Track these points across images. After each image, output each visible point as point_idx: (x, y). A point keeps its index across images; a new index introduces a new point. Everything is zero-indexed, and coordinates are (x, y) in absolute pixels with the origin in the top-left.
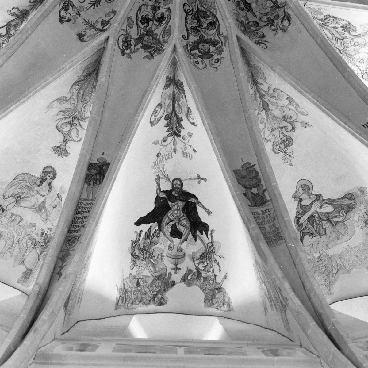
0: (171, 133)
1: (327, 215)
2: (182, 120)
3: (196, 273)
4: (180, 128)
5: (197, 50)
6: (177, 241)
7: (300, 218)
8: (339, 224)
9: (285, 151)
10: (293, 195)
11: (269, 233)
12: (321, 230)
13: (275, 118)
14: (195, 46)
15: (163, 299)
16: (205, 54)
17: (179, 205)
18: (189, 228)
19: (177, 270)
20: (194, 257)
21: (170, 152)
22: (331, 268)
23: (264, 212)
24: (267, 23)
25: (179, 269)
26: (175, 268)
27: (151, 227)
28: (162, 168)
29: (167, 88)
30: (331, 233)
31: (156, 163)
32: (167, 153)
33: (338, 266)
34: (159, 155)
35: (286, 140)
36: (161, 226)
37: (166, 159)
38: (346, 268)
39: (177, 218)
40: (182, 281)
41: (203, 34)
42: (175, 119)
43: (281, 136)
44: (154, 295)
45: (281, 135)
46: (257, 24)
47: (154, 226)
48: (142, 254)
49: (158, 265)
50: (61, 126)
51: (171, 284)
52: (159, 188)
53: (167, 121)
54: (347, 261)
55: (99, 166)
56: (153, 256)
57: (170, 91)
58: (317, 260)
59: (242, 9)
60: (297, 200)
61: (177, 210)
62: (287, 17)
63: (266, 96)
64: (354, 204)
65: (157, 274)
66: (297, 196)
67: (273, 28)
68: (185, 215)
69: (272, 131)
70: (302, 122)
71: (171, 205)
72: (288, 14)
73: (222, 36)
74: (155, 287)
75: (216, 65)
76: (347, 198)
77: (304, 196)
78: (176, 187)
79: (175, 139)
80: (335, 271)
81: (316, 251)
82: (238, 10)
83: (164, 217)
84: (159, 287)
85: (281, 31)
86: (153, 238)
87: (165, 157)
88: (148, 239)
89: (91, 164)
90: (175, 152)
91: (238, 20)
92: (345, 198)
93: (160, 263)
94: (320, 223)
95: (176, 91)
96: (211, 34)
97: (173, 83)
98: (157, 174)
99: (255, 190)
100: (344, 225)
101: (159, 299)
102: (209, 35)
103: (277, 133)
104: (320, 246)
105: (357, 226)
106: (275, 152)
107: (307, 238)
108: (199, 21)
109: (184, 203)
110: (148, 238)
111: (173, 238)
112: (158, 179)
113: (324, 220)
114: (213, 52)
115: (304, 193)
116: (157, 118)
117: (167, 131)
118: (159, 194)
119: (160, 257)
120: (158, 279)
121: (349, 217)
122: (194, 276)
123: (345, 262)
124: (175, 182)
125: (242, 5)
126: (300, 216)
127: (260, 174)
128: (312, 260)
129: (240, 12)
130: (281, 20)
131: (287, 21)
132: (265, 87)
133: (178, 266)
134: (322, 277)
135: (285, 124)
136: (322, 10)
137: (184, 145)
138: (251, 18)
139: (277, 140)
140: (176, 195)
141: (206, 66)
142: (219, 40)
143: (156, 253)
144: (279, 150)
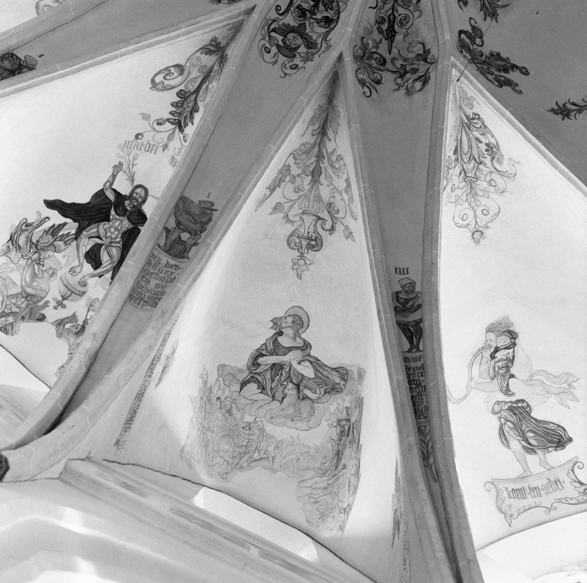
0: (175, 120)
1: (301, 378)
2: (197, 111)
3: (80, 327)
4: (188, 121)
5: (282, 38)
6: (88, 268)
7: (263, 355)
8: (307, 402)
9: (303, 252)
10: (275, 319)
11: (148, 290)
12: (280, 393)
13: (319, 198)
14: (283, 30)
15: (12, 328)
16: (287, 49)
17: (124, 223)
18: (114, 262)
19: (60, 305)
20: (93, 306)
21: (157, 144)
22: (254, 449)
23: (169, 265)
24: (397, 70)
25: (64, 307)
26: (59, 301)
27: (65, 224)
28: (133, 157)
29: (206, 54)
30: (289, 405)
31: (129, 143)
32: (152, 143)
33: (265, 454)
34: (140, 137)
35: (313, 238)
36: (81, 234)
37: (147, 149)
38: (273, 464)
39: (109, 240)
40: (55, 324)
41: (307, 25)
42: (191, 104)
43: (312, 229)
44: (5, 312)
45: (312, 227)
46: (383, 62)
47: (72, 226)
48: (29, 248)
49: (40, 280)
50: (43, 7)
51: (39, 317)
52: (111, 182)
53: (179, 99)
54: (283, 456)
55: (20, 65)
56: (42, 263)
57: (208, 60)
58: (244, 425)
59: (380, 31)
60: (276, 329)
61: (116, 229)
62: (425, 79)
63: (326, 161)
64: (342, 388)
65: (30, 291)
66: (279, 324)
67: (399, 81)
68: (121, 243)
69: (303, 213)
70: (347, 228)
71: (113, 216)
72: (429, 76)
73: (326, 43)
74: (14, 304)
75: (289, 71)
76: (338, 373)
77: (289, 332)
78: (135, 198)
79: (174, 132)
80: (256, 456)
81: (253, 413)
82: (375, 28)
83: (92, 226)
84: (20, 308)
85: (405, 91)
86: (59, 240)
87: (146, 146)
88: (51, 237)
89: (13, 54)
90: (164, 150)
91: (363, 38)
92: (337, 371)
93: (45, 279)
94: (285, 383)
95: (216, 68)
96: (315, 31)
97: (220, 54)
98: (122, 160)
99: (185, 236)
100: (312, 407)
101: (7, 323)
102: (313, 31)
103: (309, 220)
104: (262, 412)
105: (326, 420)
106: (289, 244)
107: (252, 387)
108: (316, 6)
109: (131, 226)
110: (51, 234)
111: (85, 261)
112: (118, 168)
113: (292, 382)
114: (299, 54)
115: (291, 327)
116: (166, 82)
117: (171, 113)
118: (106, 189)
119: (51, 272)
120: (26, 298)
121: (326, 400)
122: (75, 327)
123: (278, 455)
124: (139, 190)
125: (385, 27)
126: (265, 354)
127: (211, 224)
128: (237, 420)
129: (376, 32)
130: (416, 78)
131: (421, 83)
132: (330, 146)
133: (65, 302)
134: (231, 450)
135: (325, 215)
136: (475, 103)
137: (180, 147)
138: (383, 49)
139: (302, 230)
140: (129, 209)
141: (274, 63)
142: (319, 46)
143: (48, 263)
144: (297, 245)
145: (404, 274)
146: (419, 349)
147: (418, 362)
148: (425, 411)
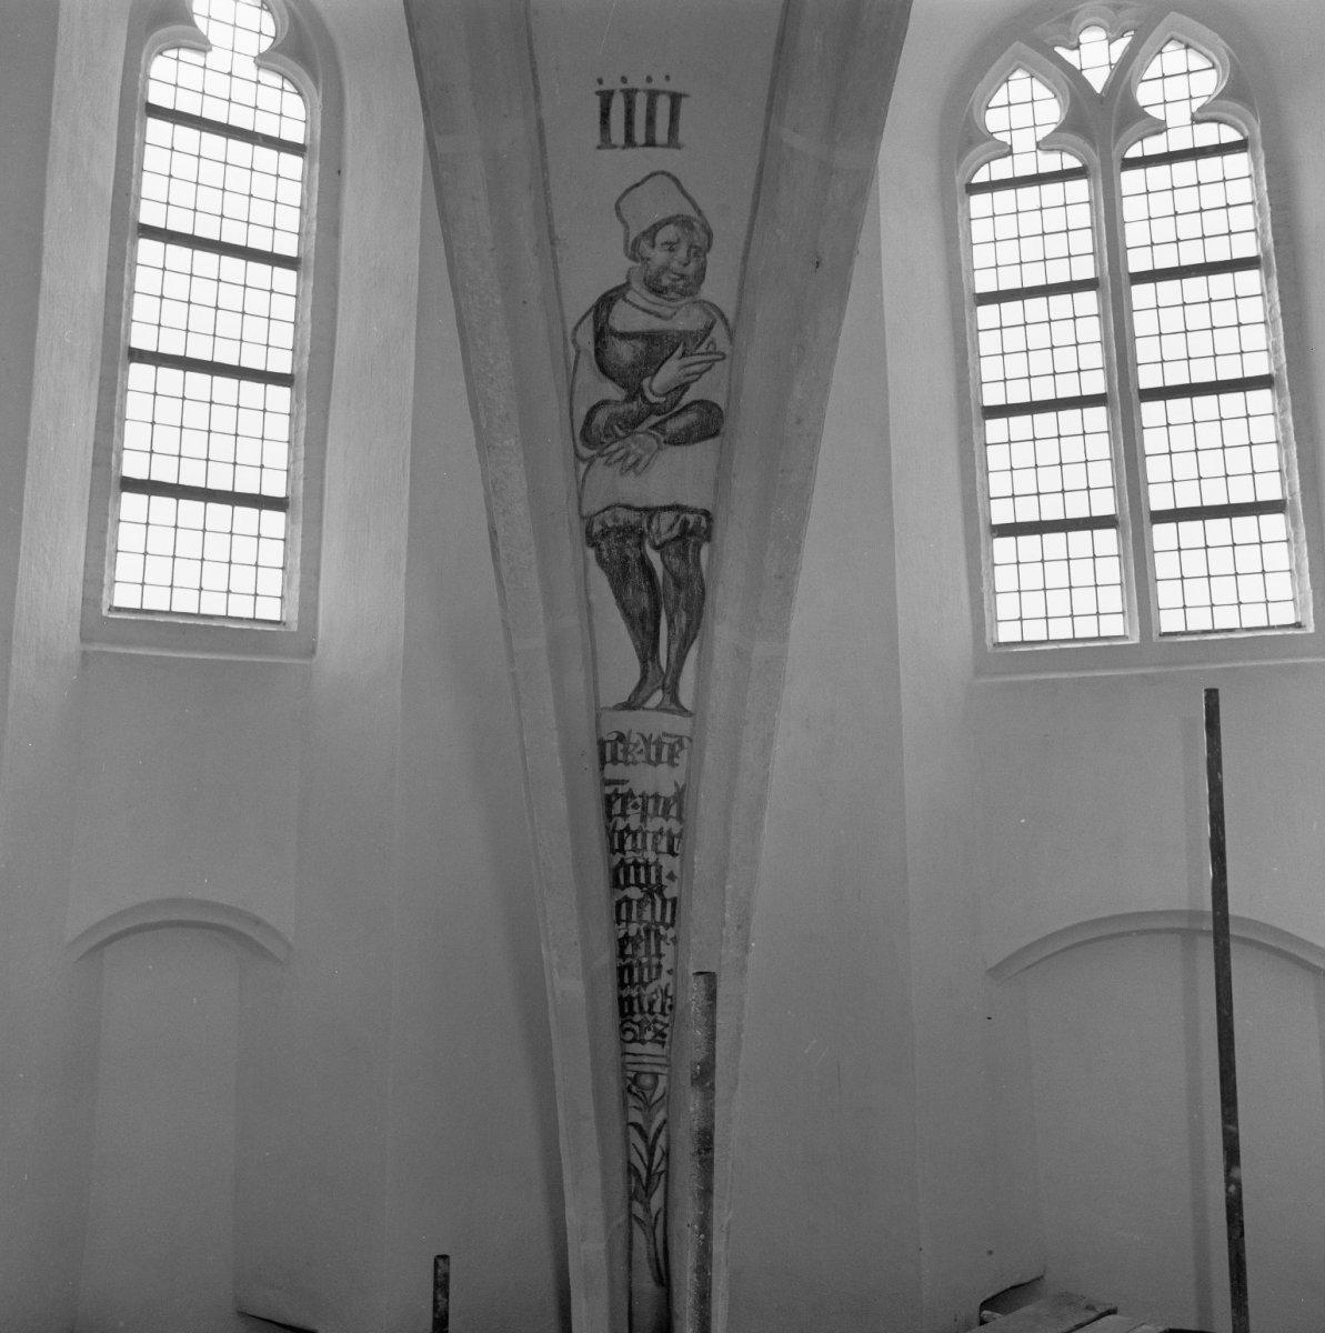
145: (651, 143)
146: (675, 699)
147: (664, 768)
148: (663, 1013)
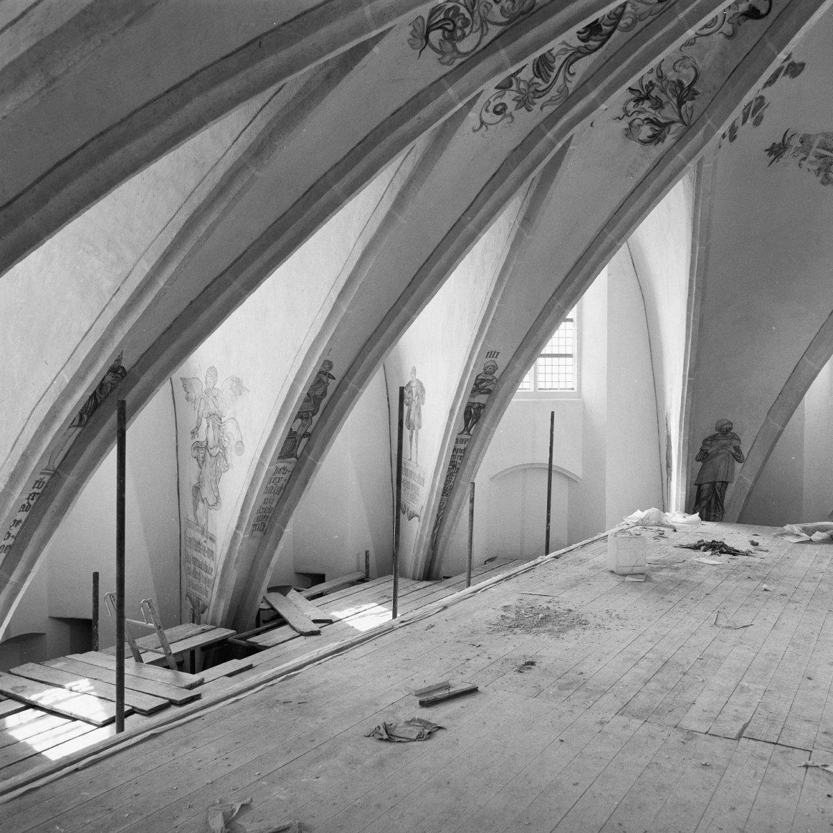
67: (631, 106)
72: (665, 137)
85: (627, 126)
127: (325, 401)
130: (652, 117)
131: (650, 133)
142: (553, 75)
